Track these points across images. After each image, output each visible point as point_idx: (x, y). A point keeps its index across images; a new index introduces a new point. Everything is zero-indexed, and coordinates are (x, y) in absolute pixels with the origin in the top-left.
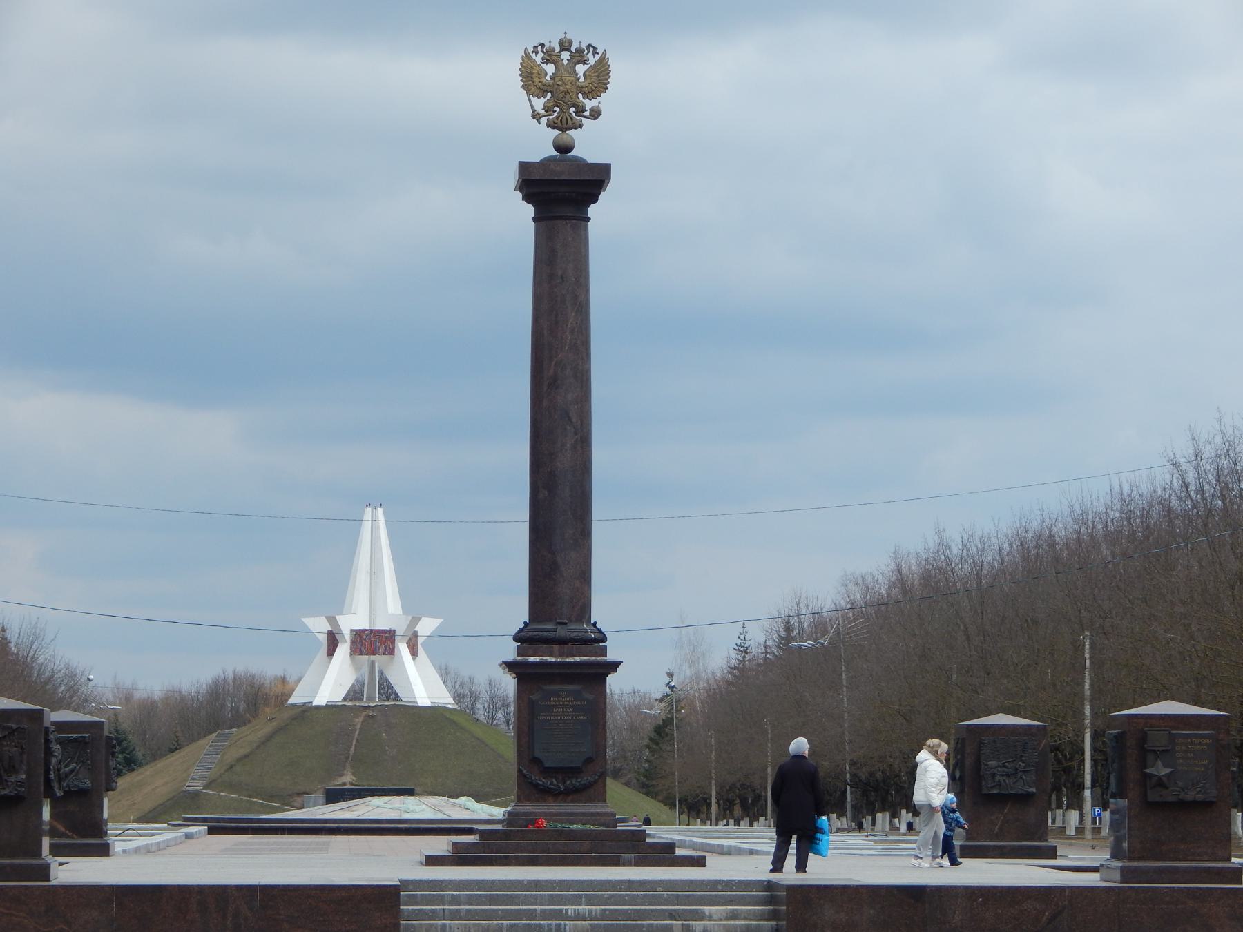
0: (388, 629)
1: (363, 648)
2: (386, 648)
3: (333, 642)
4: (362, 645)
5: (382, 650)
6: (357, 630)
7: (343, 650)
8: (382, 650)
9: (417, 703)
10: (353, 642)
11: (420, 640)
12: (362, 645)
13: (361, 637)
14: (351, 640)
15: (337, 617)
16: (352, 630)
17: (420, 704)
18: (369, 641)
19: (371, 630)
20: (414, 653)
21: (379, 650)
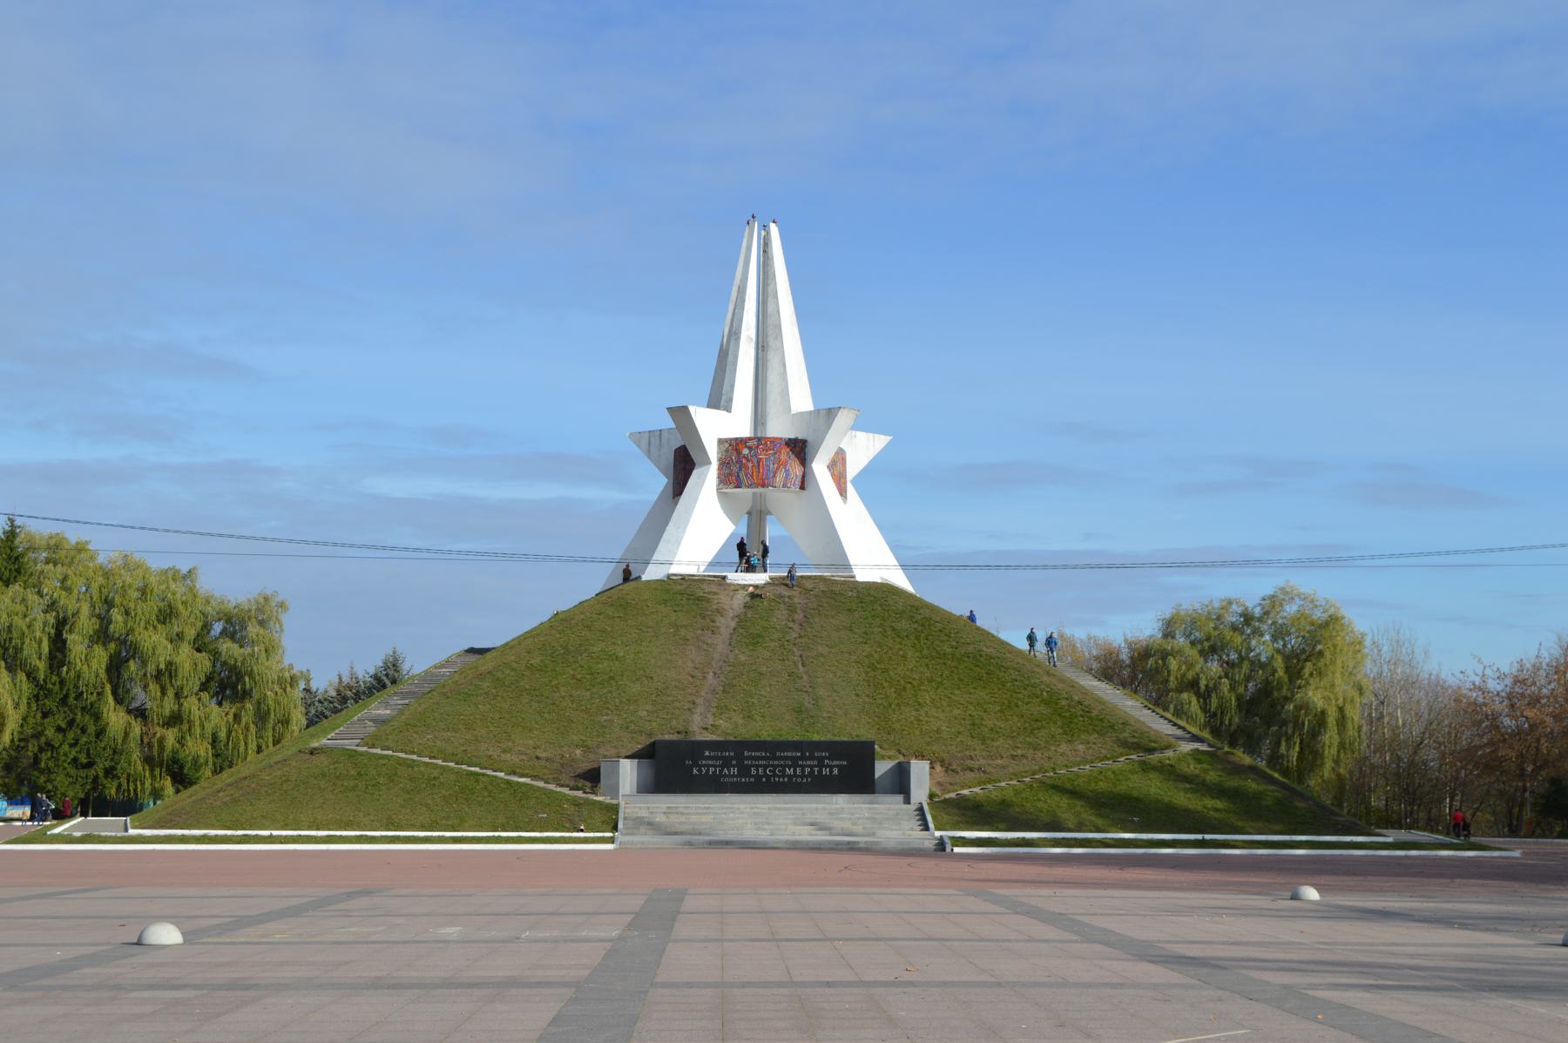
0: (792, 437)
1: (742, 474)
3: (683, 465)
4: (740, 469)
6: (731, 440)
7: (706, 482)
9: (854, 577)
10: (724, 464)
11: (853, 469)
12: (740, 469)
13: (738, 452)
14: (720, 460)
15: (692, 409)
16: (721, 442)
17: (862, 576)
18: (755, 460)
19: (759, 439)
20: (843, 492)
21: (774, 476)
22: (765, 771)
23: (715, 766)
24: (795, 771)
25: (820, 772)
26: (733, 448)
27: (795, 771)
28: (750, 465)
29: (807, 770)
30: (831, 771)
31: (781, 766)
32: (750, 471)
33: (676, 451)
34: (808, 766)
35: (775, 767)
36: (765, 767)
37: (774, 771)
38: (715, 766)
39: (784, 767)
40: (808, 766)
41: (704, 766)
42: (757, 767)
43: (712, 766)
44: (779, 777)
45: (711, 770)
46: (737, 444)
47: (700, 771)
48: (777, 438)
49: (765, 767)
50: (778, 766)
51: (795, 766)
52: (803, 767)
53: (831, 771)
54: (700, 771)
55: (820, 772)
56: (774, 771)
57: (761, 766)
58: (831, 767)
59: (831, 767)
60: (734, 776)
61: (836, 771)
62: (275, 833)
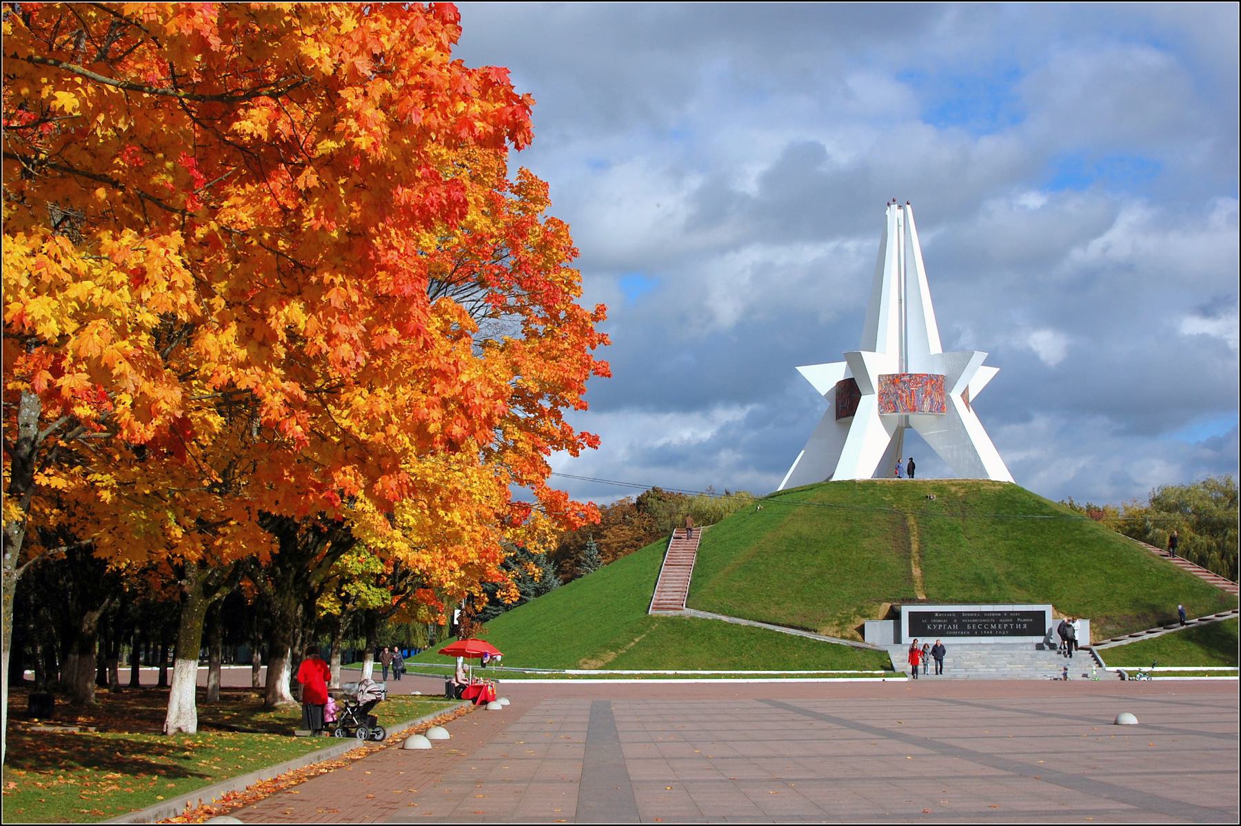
1: (898, 402)
2: (932, 400)
5: (926, 406)
8: (926, 406)
22: (977, 626)
23: (942, 624)
24: (997, 626)
25: (1014, 626)
26: (892, 381)
27: (997, 626)
28: (904, 395)
29: (1006, 625)
30: (1022, 626)
31: (988, 623)
32: (904, 399)
33: (839, 384)
34: (1005, 623)
35: (984, 623)
36: (977, 624)
37: (982, 627)
38: (942, 624)
39: (990, 623)
40: (1005, 623)
41: (935, 623)
42: (971, 624)
43: (940, 623)
44: (987, 630)
45: (940, 626)
46: (894, 379)
47: (932, 627)
48: (924, 375)
49: (977, 624)
50: (986, 623)
51: (997, 623)
52: (1003, 624)
53: (1022, 626)
54: (932, 627)
55: (1014, 626)
56: (982, 627)
57: (973, 623)
58: (1022, 624)
59: (1022, 624)
60: (955, 630)
61: (1025, 626)
62: (678, 672)
